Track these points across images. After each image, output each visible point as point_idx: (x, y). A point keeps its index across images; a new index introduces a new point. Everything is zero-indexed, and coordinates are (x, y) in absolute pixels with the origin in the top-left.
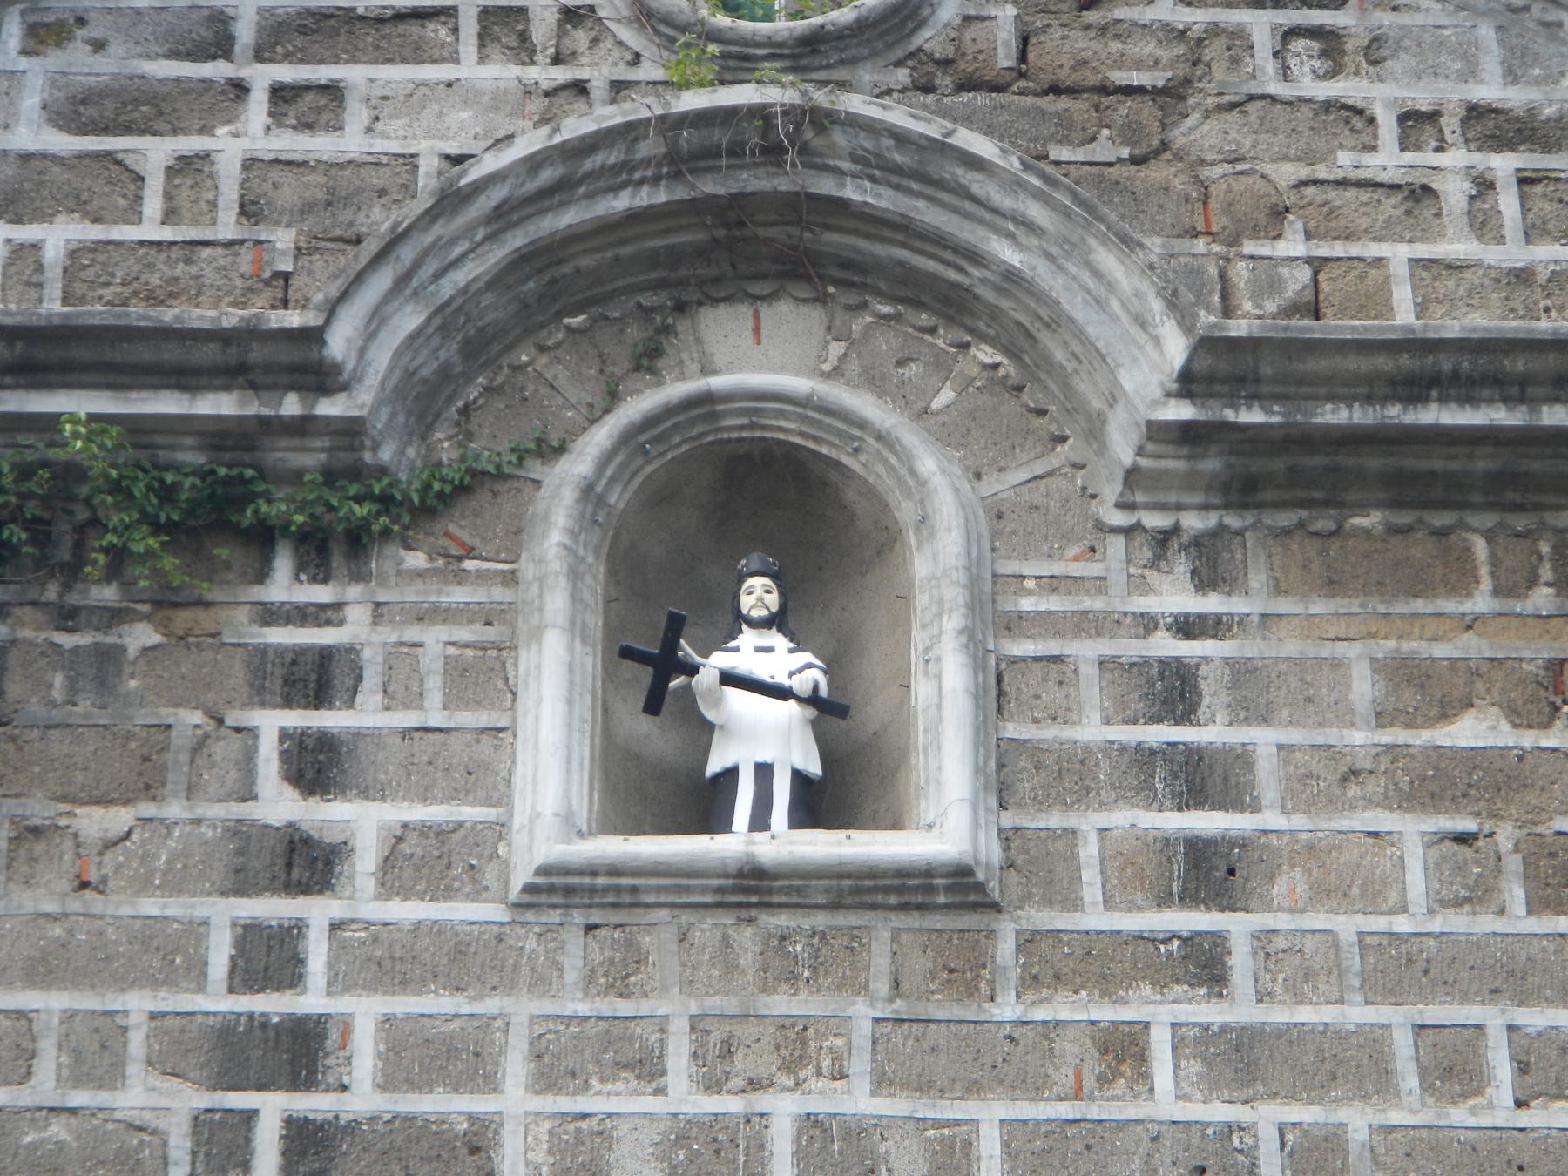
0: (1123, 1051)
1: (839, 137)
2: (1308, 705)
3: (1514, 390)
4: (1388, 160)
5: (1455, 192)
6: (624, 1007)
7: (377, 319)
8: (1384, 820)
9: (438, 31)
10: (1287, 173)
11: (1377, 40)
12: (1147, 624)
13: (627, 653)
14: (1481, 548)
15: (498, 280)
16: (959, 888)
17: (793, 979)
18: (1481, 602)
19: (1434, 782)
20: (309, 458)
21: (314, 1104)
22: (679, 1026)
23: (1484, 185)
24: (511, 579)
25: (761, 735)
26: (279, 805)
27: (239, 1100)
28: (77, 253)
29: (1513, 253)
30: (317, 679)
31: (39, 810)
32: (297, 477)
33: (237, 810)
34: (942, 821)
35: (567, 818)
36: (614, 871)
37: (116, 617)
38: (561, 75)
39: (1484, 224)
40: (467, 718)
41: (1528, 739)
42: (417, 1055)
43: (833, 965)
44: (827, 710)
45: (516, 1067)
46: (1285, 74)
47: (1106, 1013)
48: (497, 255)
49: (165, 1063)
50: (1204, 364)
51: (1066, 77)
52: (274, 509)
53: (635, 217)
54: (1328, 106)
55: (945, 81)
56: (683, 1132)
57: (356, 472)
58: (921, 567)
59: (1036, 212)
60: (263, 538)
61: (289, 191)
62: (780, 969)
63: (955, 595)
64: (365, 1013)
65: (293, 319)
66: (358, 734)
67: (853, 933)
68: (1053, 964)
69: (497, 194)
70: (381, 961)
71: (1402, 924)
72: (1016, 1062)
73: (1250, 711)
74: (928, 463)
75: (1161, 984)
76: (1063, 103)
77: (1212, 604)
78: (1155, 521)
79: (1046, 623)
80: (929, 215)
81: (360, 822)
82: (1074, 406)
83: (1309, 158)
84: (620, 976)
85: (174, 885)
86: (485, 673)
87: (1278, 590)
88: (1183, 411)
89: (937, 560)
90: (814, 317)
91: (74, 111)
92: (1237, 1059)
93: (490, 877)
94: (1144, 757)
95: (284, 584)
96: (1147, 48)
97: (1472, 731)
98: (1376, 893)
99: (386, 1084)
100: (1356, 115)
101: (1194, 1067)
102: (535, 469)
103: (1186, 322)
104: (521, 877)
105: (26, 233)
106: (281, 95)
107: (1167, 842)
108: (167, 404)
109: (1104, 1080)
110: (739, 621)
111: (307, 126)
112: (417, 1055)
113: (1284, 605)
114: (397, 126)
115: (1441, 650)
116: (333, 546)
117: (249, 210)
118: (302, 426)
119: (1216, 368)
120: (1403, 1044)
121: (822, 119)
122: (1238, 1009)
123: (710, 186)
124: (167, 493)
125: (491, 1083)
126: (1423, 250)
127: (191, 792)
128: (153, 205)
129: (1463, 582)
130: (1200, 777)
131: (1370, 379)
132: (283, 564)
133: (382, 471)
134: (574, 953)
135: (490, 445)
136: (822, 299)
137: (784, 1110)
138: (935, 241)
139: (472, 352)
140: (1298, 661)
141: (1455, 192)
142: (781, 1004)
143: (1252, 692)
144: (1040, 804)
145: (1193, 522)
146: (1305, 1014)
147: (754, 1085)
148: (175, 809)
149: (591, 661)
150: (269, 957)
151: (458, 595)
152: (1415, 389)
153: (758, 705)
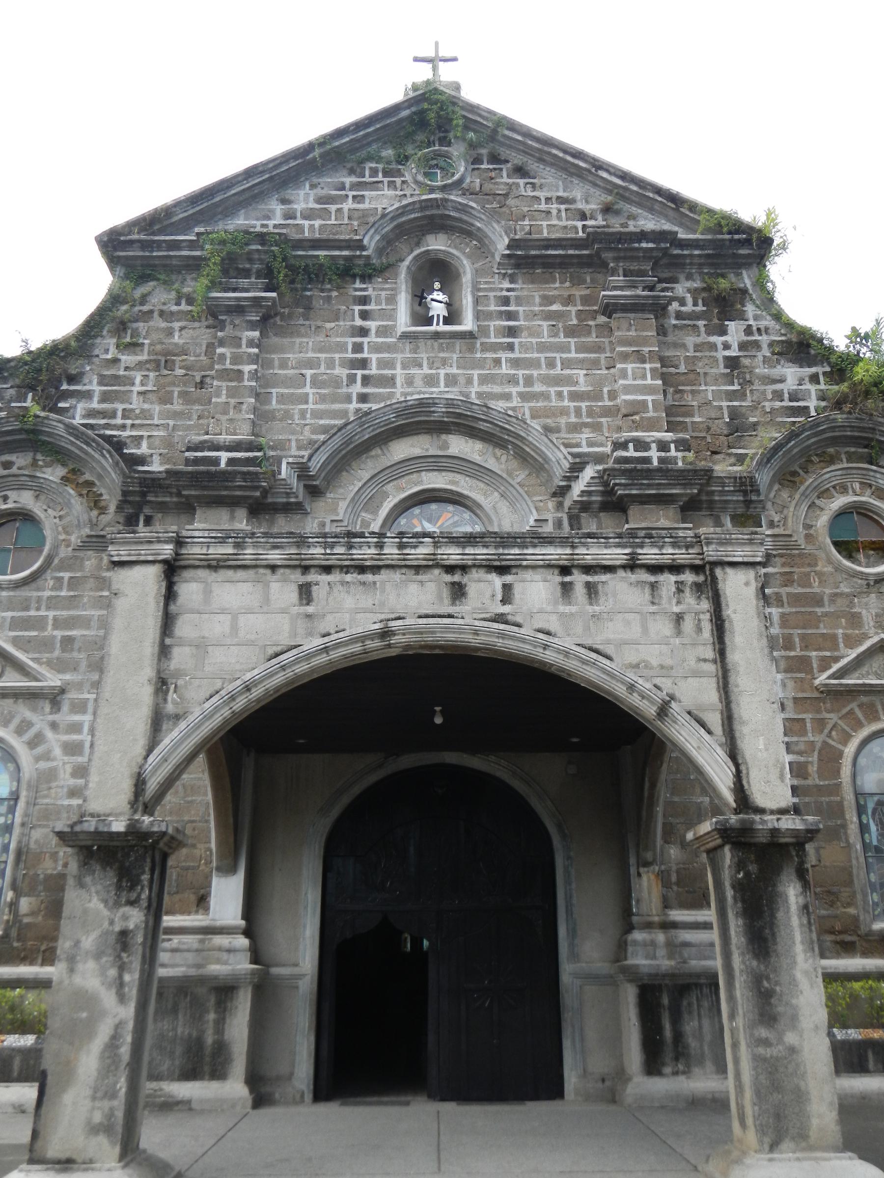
0: (497, 362)
1: (449, 204)
2: (529, 303)
3: (564, 247)
4: (543, 206)
5: (554, 212)
6: (416, 356)
7: (372, 237)
8: (541, 323)
9: (381, 185)
10: (526, 209)
11: (541, 185)
12: (502, 289)
13: (416, 296)
14: (557, 275)
15: (392, 230)
16: (469, 336)
17: (443, 351)
18: (557, 285)
19: (549, 316)
20: (361, 262)
21: (366, 372)
22: (425, 359)
23: (559, 211)
24: (396, 283)
25: (438, 309)
26: (359, 322)
27: (354, 372)
28: (321, 226)
29: (564, 223)
30: (364, 300)
31: (319, 323)
32: (359, 265)
33: (352, 323)
34: (468, 324)
35: (406, 324)
36: (414, 333)
37: (330, 290)
38: (402, 193)
39: (559, 218)
40: (389, 307)
41: (564, 308)
42: (382, 364)
43: (450, 348)
44: (448, 305)
45: (399, 366)
46: (526, 191)
47: (495, 356)
48: (392, 226)
49: (342, 365)
50: (511, 243)
51: (488, 192)
52: (357, 271)
53: (415, 219)
54: (533, 197)
55: (467, 193)
56: (426, 376)
57: (369, 264)
58: (464, 280)
59: (483, 217)
60: (354, 276)
61: (356, 215)
62: (441, 349)
63: (470, 285)
64: (374, 357)
65: (358, 237)
66: (371, 310)
67: (453, 343)
68: (486, 348)
69: (391, 215)
70: (377, 348)
71: (543, 340)
72: (480, 364)
73: (518, 305)
74: (465, 262)
75: (503, 351)
76: (488, 197)
77: (512, 286)
78: (503, 271)
79: (485, 290)
80: (465, 218)
81: (372, 325)
82: (489, 251)
83: (530, 206)
84: (415, 351)
85: (342, 336)
86: (392, 300)
87: (524, 283)
88: (507, 252)
89: (467, 279)
90: (446, 236)
91: (319, 200)
92: (516, 363)
93: (394, 334)
94: (501, 312)
95: (358, 285)
96: (502, 187)
97: (554, 307)
98: (539, 335)
100: (537, 198)
101: (508, 364)
102: (399, 264)
103: (508, 237)
104: (399, 334)
105: (312, 222)
106: (354, 197)
107: (505, 327)
108: (337, 253)
109: (494, 367)
110: (434, 290)
111: (359, 203)
112: (382, 364)
113: (524, 286)
114: (374, 203)
115: (550, 293)
116: (366, 278)
117: (349, 218)
118: (360, 256)
120: (543, 360)
121: (447, 200)
122: (516, 355)
123: (428, 213)
124: (338, 269)
125: (395, 369)
126: (549, 223)
127: (344, 320)
128: (333, 217)
129: (554, 282)
130: (511, 316)
131: (539, 246)
132: (358, 281)
133: (374, 264)
134: (408, 347)
135: (392, 259)
136: (447, 233)
137: (442, 372)
138: (466, 222)
139: (388, 243)
140: (527, 296)
141: (554, 212)
142: (442, 355)
143: (519, 301)
144: (484, 320)
145: (509, 272)
146: (527, 356)
147: (438, 368)
148: (341, 323)
149: (409, 297)
150: (358, 348)
151: (387, 286)
152: (547, 247)
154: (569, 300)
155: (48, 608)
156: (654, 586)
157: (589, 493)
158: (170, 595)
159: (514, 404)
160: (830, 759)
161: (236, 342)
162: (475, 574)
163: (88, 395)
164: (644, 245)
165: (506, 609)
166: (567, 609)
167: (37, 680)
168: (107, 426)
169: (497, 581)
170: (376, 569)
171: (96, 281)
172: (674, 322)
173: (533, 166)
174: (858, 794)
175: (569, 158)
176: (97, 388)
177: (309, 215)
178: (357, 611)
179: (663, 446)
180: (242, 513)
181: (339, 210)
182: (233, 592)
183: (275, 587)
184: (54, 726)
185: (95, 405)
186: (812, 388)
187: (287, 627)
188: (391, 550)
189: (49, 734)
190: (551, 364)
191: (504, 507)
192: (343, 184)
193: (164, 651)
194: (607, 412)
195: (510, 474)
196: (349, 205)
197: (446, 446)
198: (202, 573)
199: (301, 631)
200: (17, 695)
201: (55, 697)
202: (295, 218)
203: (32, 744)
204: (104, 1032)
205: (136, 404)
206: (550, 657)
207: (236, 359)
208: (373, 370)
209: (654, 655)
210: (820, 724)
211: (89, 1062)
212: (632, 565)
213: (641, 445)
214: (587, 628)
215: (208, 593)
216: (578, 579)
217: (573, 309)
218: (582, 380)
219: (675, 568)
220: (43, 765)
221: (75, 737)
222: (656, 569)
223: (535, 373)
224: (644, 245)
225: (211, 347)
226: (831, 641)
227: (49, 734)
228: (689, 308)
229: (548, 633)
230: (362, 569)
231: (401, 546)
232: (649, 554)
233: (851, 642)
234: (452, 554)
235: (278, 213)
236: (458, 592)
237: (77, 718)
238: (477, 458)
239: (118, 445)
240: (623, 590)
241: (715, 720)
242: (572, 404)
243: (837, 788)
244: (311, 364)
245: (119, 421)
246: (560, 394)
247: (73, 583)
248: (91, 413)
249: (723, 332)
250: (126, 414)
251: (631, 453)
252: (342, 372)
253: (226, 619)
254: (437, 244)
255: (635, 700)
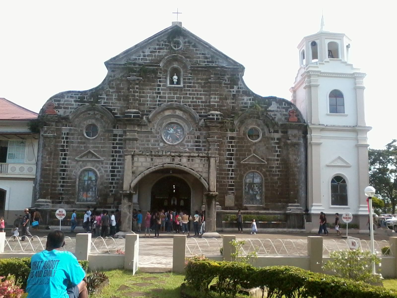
4: (199, 56)
5: (201, 57)
18: (200, 76)
19: (198, 83)
25: (175, 81)
26: (159, 83)
30: (160, 78)
34: (182, 85)
39: (202, 59)
44: (177, 80)
49: (155, 93)
64: (162, 92)
70: (162, 90)
81: (162, 84)
86: (166, 78)
89: (182, 73)
99: (163, 94)
106: (158, 51)
119: (191, 67)
130: (190, 83)
137: (176, 96)
143: (192, 79)
150: (159, 89)
153: (175, 77)
154: (202, 80)
155: (100, 144)
156: (201, 160)
157: (203, 124)
158: (133, 159)
159: (190, 103)
160: (241, 177)
161: (133, 88)
162: (176, 157)
163: (104, 98)
164: (218, 69)
165: (180, 163)
166: (189, 163)
167: (99, 158)
168: (108, 106)
169: (179, 158)
170: (161, 156)
171: (104, 73)
172: (223, 85)
173: (197, 44)
174: (246, 183)
175: (205, 45)
176: (105, 97)
177: (148, 56)
178: (159, 162)
179: (217, 115)
180: (136, 126)
181: (155, 55)
182: (142, 159)
183: (148, 159)
184: (102, 167)
185: (105, 101)
186: (249, 102)
187: (149, 165)
188: (164, 153)
189: (102, 169)
190: (198, 94)
191: (186, 126)
192: (156, 48)
193: (133, 168)
194: (208, 106)
195: (187, 119)
196: (157, 54)
197: (175, 112)
198: (137, 156)
199: (151, 165)
200: (95, 161)
201: (102, 162)
202: (145, 57)
203: (99, 170)
204: (128, 217)
205: (114, 101)
206: (185, 170)
207: (134, 92)
208: (162, 95)
209: (200, 170)
210: (240, 170)
211: (127, 220)
212: (198, 156)
213: (213, 115)
214: (191, 166)
215: (138, 159)
216: (191, 158)
217: (203, 82)
218: (203, 98)
219: (204, 157)
220: (101, 174)
221: (106, 169)
222: (202, 157)
223: (194, 96)
224: (218, 69)
225: (128, 89)
226: (244, 155)
227: (102, 169)
228: (227, 82)
229: (186, 167)
230: (160, 156)
231: (166, 153)
232: (201, 155)
233: (248, 155)
234: (173, 154)
235: (142, 56)
236: (173, 160)
237: (106, 166)
238: (181, 115)
239: (111, 110)
240: (197, 160)
241: (207, 180)
242: (201, 104)
243: (242, 182)
244: (149, 93)
245: (111, 105)
246: (199, 102)
247: (104, 140)
248: (105, 103)
249: (233, 88)
250: (112, 103)
251: (211, 117)
252: (155, 95)
253: (141, 163)
254: (176, 65)
255: (196, 176)
